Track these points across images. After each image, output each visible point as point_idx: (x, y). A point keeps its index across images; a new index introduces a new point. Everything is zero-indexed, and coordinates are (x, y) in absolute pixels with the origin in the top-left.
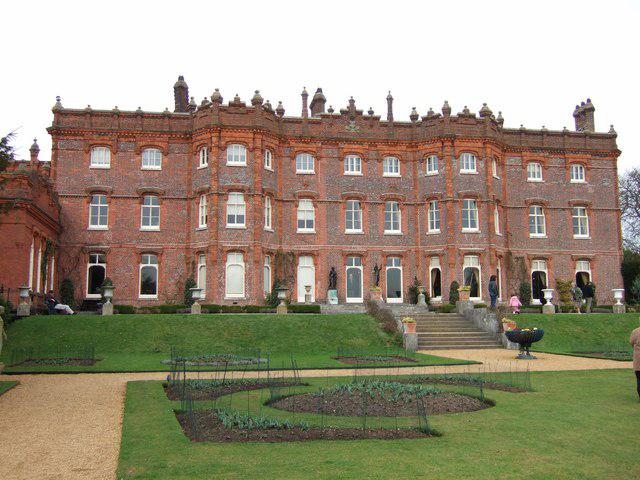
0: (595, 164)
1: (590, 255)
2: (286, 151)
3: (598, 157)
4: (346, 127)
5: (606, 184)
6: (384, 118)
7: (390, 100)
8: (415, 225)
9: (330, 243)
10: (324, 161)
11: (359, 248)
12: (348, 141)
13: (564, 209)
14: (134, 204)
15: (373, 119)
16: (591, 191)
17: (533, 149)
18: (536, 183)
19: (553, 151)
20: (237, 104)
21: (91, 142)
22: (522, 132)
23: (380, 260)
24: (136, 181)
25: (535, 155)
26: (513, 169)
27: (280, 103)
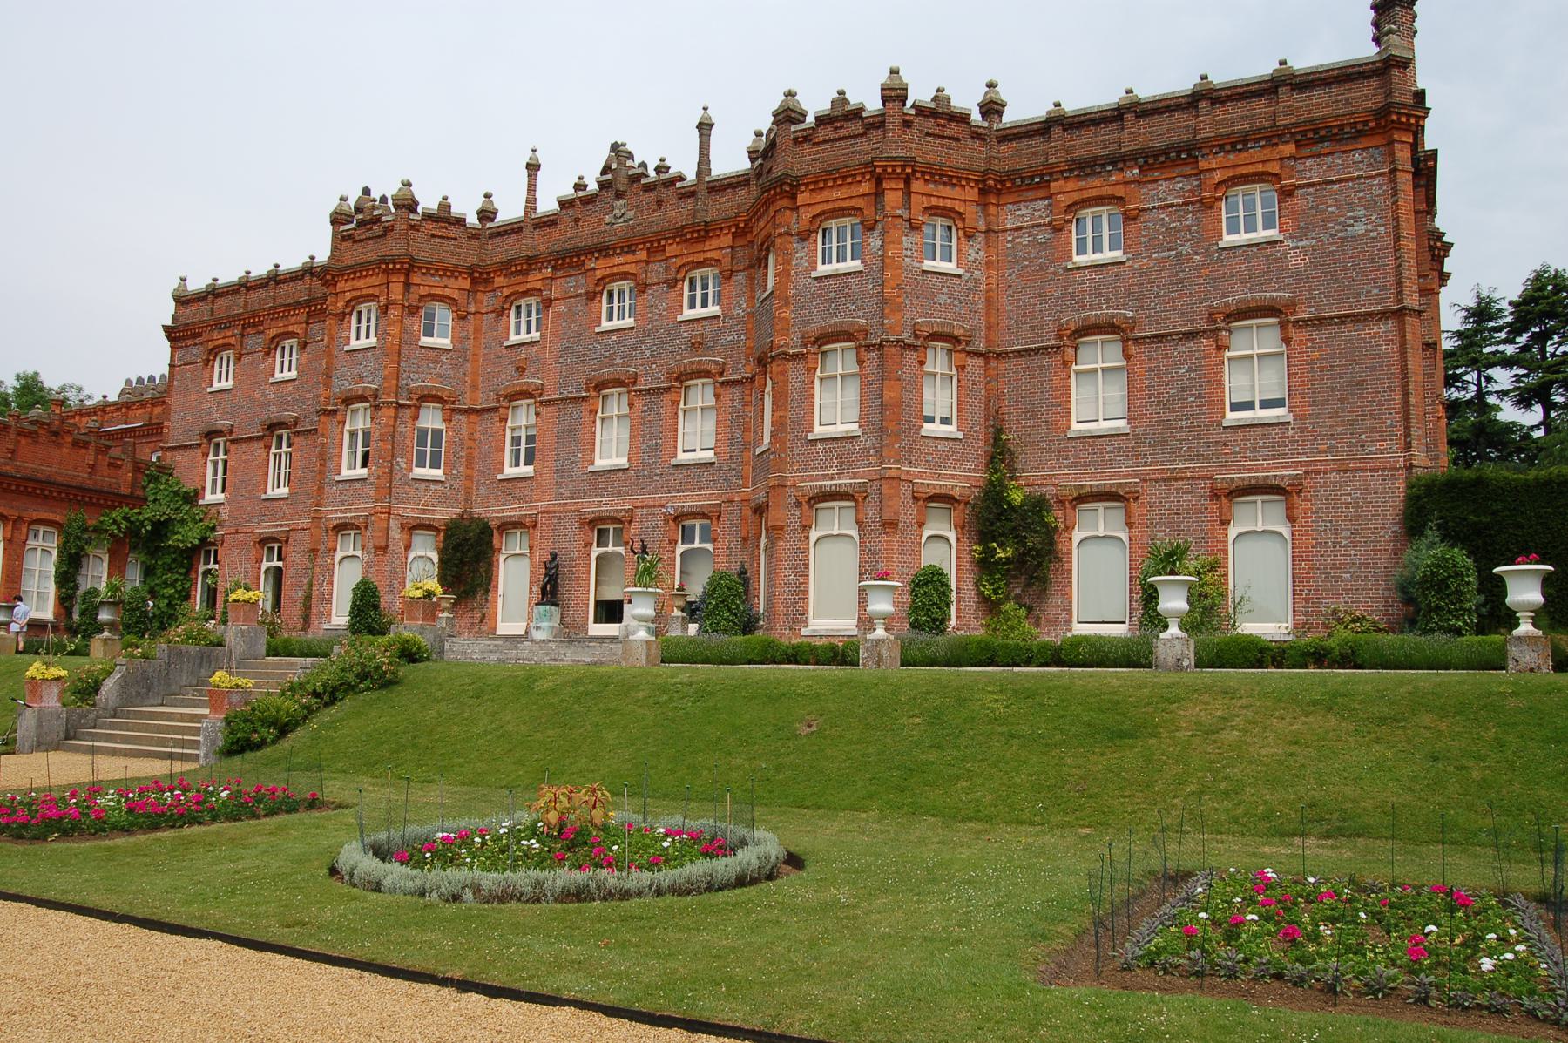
0: (1313, 170)
1: (1284, 475)
2: (488, 301)
3: (1326, 147)
4: (608, 219)
5: (1359, 229)
6: (691, 176)
7: (705, 127)
8: (737, 429)
9: (560, 496)
10: (560, 307)
11: (616, 504)
12: (603, 250)
13: (1191, 335)
14: (258, 447)
15: (668, 182)
16: (1297, 260)
17: (1086, 167)
18: (1096, 267)
19: (1155, 161)
20: (444, 218)
21: (211, 345)
22: (1058, 123)
23: (662, 530)
24: (263, 405)
25: (1095, 186)
26: (1025, 240)
27: (488, 196)
